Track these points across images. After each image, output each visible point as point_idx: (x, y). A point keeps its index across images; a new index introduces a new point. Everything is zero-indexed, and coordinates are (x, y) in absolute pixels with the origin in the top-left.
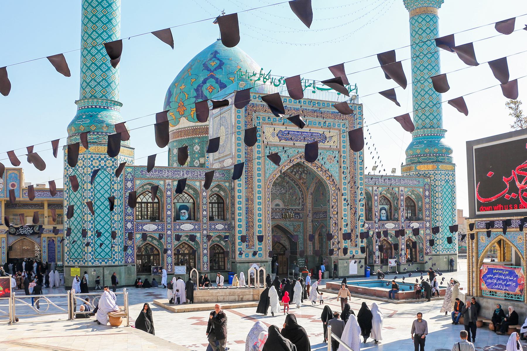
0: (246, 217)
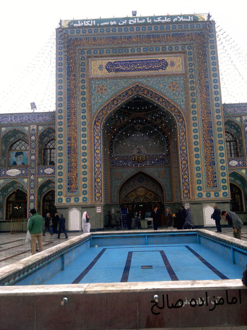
0: (68, 157)
